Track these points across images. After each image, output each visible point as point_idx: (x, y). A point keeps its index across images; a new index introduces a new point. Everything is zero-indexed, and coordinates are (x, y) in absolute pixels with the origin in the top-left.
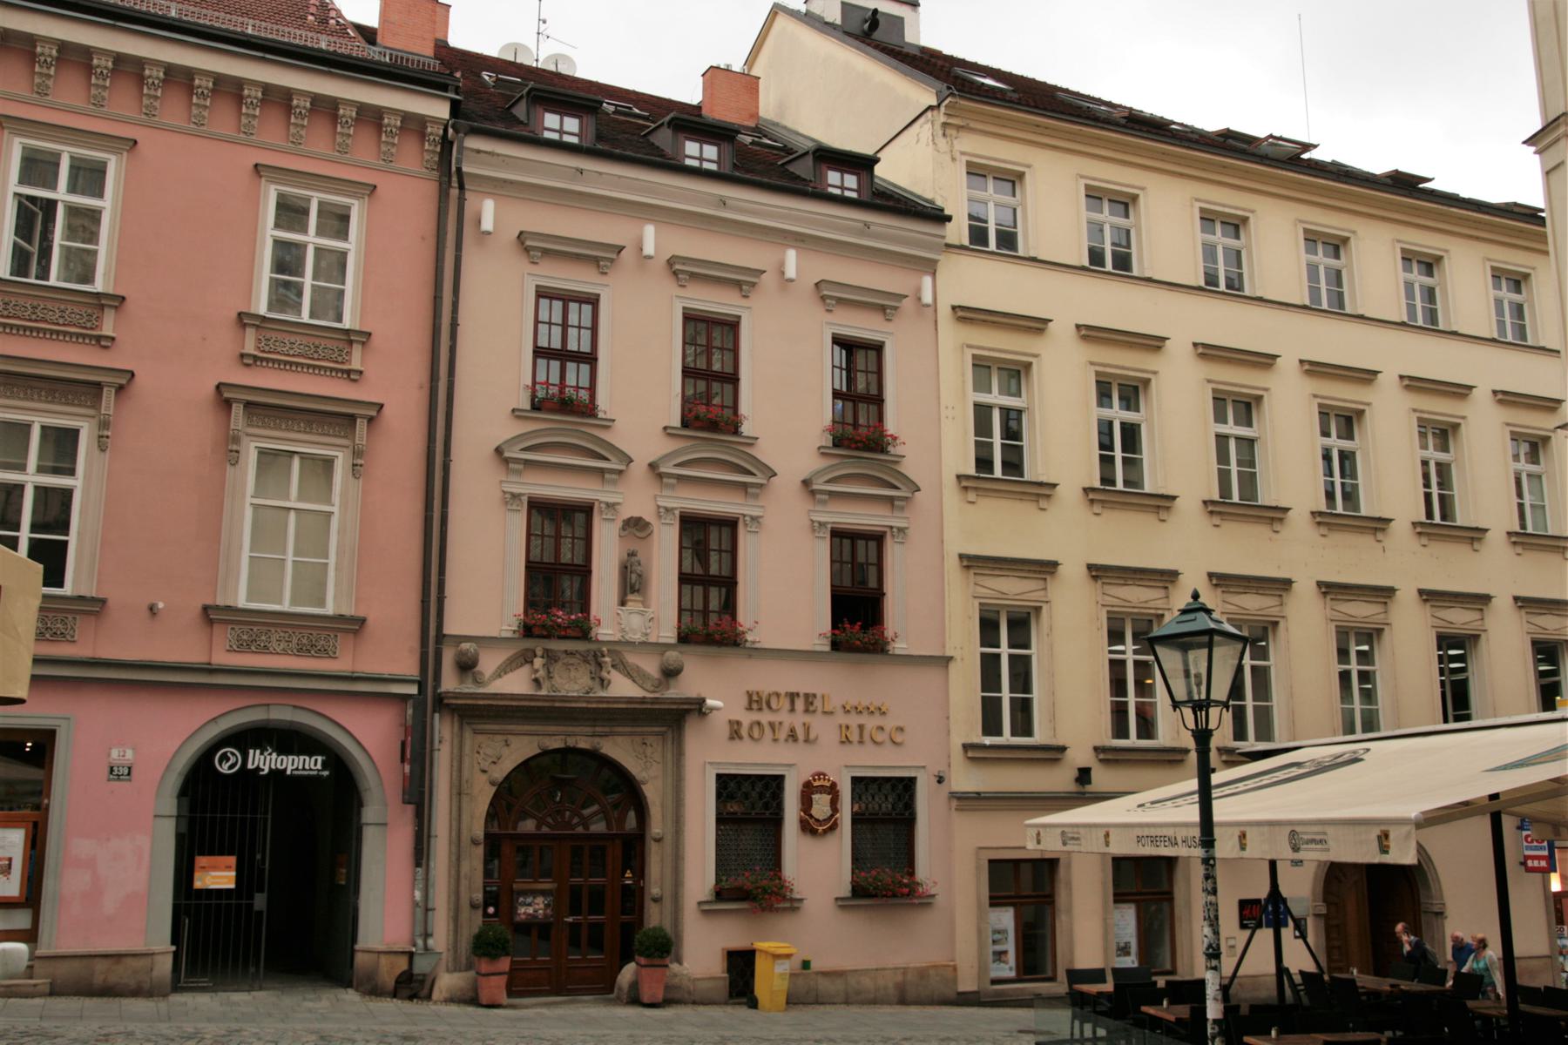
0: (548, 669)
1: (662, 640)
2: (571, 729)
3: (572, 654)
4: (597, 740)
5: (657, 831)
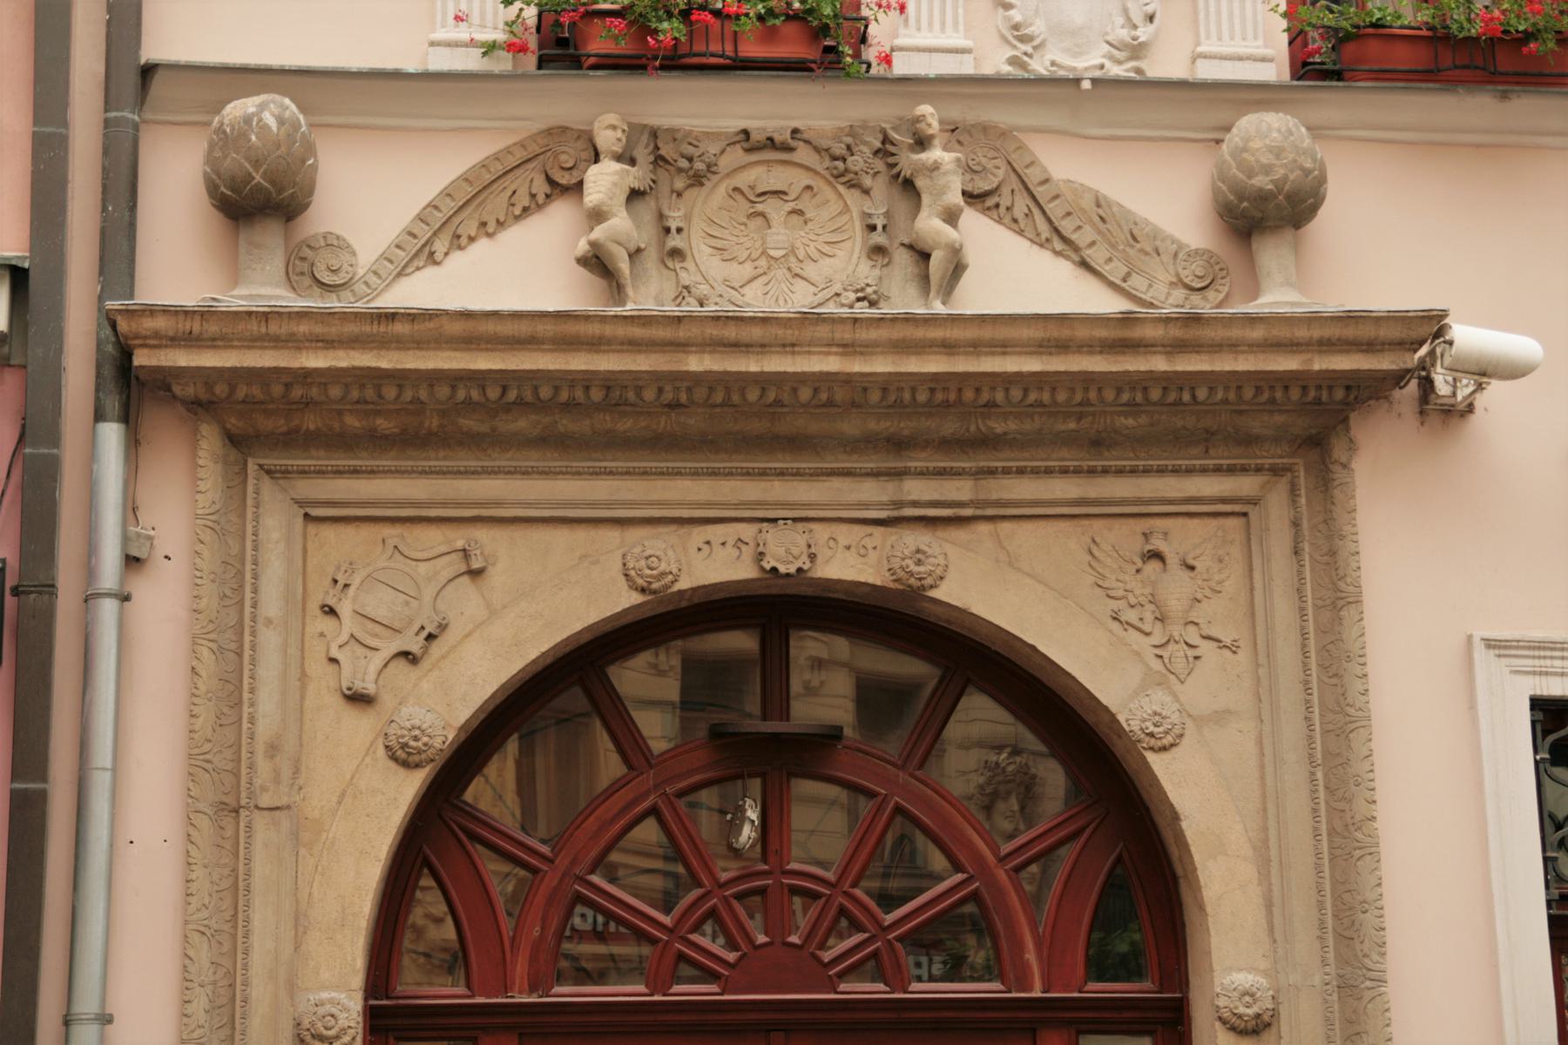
0: (661, 216)
1: (1208, 71)
2: (778, 490)
3: (771, 143)
4: (912, 539)
5: (1243, 979)
